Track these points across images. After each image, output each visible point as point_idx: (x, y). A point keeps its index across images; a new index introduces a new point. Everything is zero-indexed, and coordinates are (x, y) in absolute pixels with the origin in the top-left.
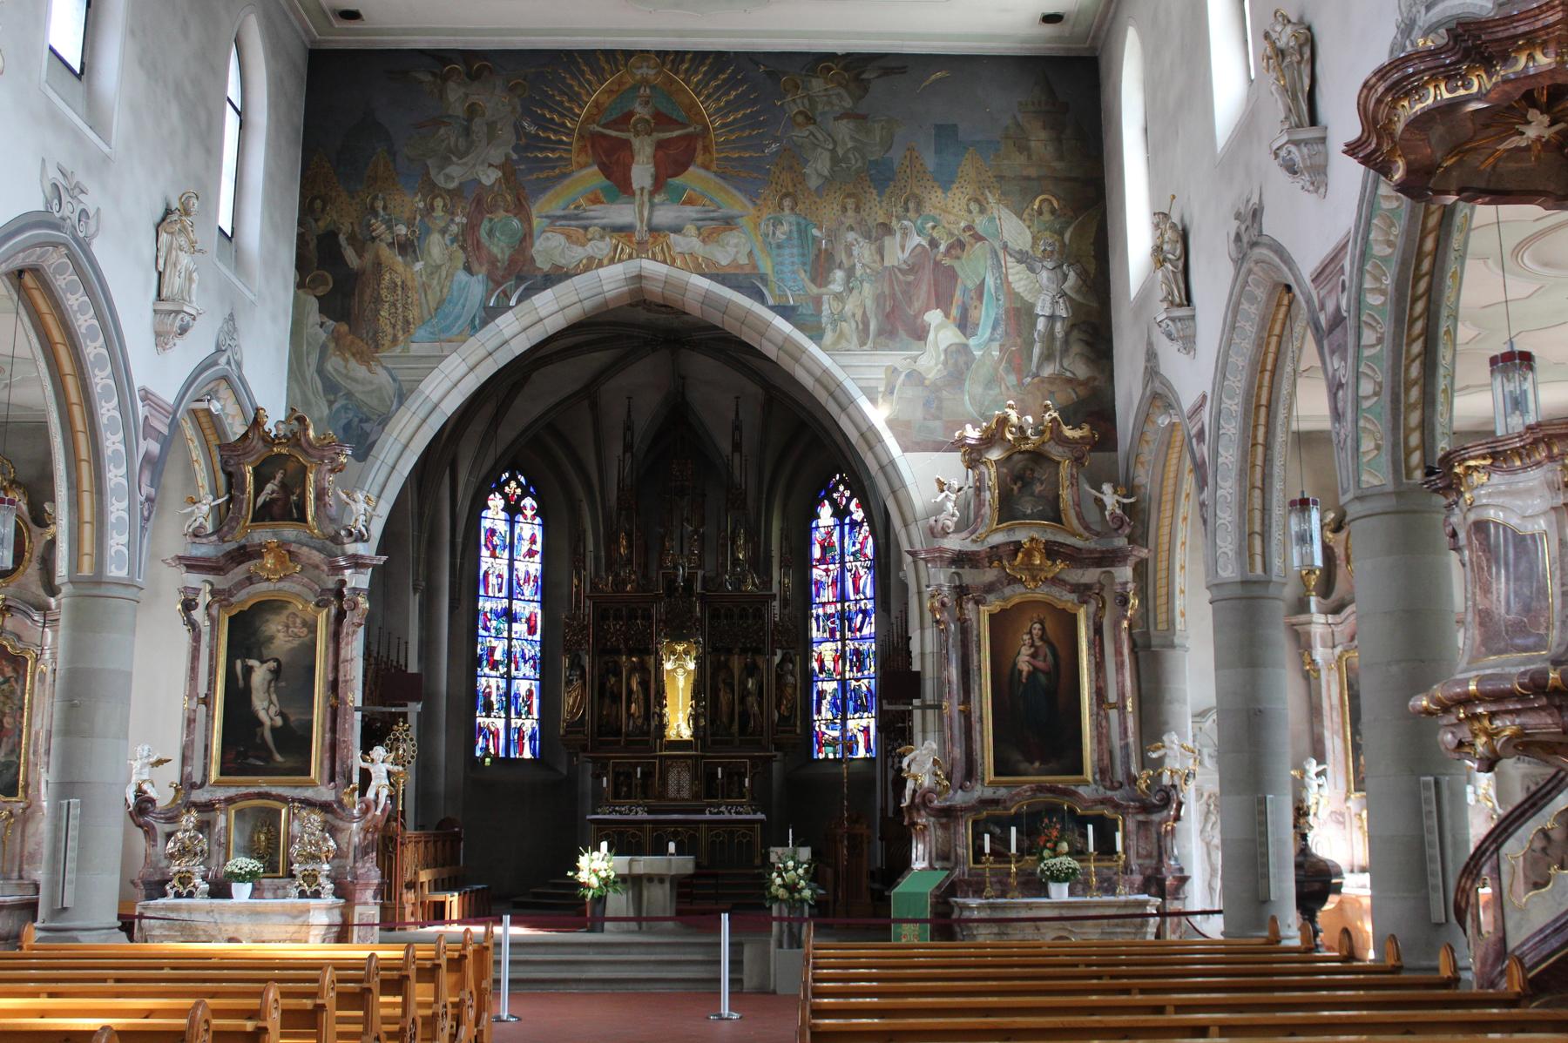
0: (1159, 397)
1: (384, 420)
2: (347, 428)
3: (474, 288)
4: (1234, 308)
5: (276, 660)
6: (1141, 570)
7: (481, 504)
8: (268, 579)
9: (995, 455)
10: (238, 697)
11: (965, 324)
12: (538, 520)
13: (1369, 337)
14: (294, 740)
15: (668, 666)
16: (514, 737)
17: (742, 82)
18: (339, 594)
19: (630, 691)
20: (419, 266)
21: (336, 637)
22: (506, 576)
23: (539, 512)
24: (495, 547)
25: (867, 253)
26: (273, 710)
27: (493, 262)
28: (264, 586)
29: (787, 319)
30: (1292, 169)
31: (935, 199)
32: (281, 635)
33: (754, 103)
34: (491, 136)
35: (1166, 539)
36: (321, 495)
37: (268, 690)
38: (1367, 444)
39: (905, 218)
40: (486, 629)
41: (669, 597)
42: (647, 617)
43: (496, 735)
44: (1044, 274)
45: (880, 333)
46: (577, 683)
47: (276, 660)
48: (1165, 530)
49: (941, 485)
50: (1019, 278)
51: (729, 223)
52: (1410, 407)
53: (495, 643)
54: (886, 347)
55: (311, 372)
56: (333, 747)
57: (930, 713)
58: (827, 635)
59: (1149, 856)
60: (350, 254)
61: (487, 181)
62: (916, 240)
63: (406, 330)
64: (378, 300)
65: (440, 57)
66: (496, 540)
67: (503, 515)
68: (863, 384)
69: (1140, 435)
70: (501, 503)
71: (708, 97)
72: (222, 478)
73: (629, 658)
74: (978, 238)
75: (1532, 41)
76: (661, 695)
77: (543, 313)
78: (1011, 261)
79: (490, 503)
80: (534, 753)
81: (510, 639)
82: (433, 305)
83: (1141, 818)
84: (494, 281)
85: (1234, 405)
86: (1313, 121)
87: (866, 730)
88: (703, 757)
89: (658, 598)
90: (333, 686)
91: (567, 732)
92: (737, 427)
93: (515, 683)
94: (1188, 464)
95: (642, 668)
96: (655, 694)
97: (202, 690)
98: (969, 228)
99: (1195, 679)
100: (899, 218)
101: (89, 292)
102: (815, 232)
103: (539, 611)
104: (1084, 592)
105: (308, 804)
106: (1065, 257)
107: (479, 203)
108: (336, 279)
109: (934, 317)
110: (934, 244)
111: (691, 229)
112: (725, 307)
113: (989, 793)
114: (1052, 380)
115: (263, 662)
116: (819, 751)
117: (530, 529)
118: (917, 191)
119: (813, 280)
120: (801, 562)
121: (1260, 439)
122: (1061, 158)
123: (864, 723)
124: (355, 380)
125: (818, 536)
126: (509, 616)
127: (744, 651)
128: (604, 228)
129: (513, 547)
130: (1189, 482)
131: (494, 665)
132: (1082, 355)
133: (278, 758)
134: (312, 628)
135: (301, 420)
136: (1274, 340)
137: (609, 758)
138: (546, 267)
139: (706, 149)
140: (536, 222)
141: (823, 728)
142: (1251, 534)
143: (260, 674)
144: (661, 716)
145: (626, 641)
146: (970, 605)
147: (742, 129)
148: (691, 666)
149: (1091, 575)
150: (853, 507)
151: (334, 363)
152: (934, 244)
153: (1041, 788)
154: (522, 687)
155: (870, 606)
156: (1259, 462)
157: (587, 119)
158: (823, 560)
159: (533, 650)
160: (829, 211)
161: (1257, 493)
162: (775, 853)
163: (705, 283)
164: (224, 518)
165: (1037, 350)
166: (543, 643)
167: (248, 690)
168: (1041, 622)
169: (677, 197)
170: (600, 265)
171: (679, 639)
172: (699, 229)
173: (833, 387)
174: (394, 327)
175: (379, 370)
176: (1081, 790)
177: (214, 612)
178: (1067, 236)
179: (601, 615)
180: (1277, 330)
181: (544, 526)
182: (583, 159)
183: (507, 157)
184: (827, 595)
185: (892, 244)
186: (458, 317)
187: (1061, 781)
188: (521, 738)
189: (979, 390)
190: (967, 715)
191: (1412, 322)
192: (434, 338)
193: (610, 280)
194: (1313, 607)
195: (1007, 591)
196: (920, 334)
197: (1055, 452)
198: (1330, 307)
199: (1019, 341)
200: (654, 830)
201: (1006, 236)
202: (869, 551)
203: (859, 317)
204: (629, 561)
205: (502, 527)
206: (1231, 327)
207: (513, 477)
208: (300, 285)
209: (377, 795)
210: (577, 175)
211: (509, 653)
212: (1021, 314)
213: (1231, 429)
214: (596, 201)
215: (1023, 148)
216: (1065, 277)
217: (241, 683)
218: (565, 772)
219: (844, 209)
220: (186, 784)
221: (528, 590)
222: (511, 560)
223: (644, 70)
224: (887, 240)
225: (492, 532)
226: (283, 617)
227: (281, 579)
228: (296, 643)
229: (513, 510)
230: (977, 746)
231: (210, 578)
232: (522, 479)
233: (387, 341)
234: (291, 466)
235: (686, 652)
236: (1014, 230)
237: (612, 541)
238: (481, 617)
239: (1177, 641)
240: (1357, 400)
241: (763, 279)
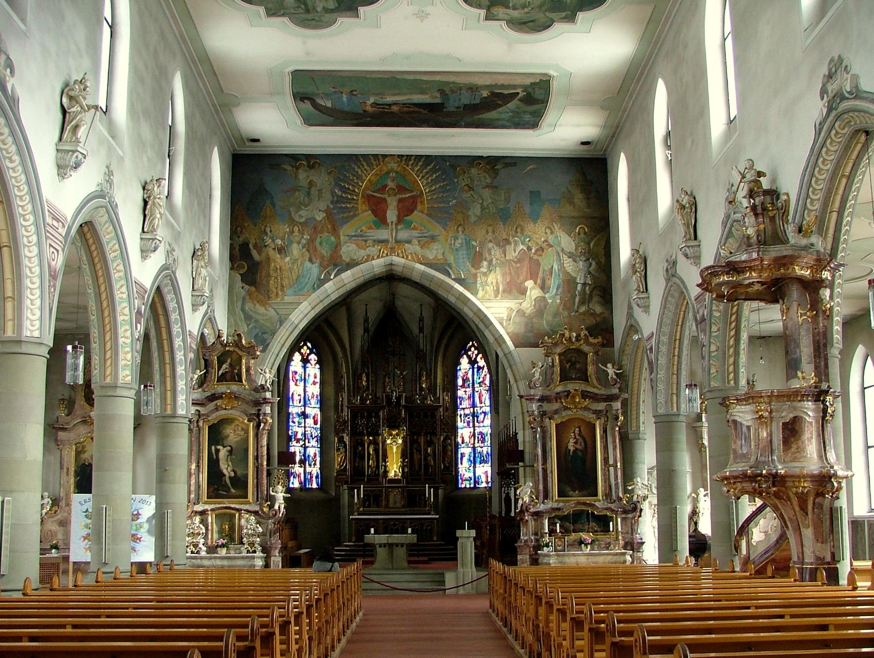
0: (633, 328)
1: (273, 333)
2: (256, 337)
3: (314, 270)
4: (665, 299)
6: (625, 404)
9: (559, 350)
10: (213, 463)
11: (544, 287)
12: (318, 366)
13: (714, 328)
14: (240, 483)
15: (389, 442)
16: (308, 477)
17: (437, 171)
18: (258, 415)
19: (369, 454)
20: (288, 259)
21: (257, 436)
23: (319, 362)
25: (498, 253)
26: (229, 469)
27: (323, 257)
28: (223, 412)
29: (461, 285)
30: (686, 256)
31: (530, 227)
33: (444, 180)
34: (320, 197)
35: (636, 389)
36: (248, 370)
38: (713, 370)
39: (516, 236)
40: (294, 422)
41: (389, 407)
43: (299, 476)
44: (581, 263)
45: (504, 291)
48: (636, 385)
49: (534, 365)
50: (569, 265)
51: (433, 239)
52: (730, 356)
54: (507, 298)
55: (238, 310)
56: (258, 485)
57: (528, 469)
58: (466, 424)
59: (627, 533)
60: (254, 253)
61: (319, 219)
62: (522, 247)
63: (282, 291)
64: (268, 276)
65: (294, 158)
66: (297, 377)
67: (301, 364)
68: (497, 316)
69: (624, 343)
71: (423, 177)
72: (203, 362)
73: (368, 438)
74: (552, 246)
75: (751, 269)
76: (385, 456)
77: (346, 282)
78: (565, 258)
81: (305, 427)
82: (295, 277)
83: (623, 516)
84: (323, 267)
85: (664, 339)
86: (696, 238)
89: (383, 408)
90: (257, 458)
91: (338, 475)
92: (421, 320)
93: (308, 450)
94: (646, 365)
95: (375, 443)
96: (382, 455)
98: (546, 241)
99: (647, 456)
100: (513, 237)
101: (175, 293)
102: (474, 243)
103: (319, 413)
104: (598, 413)
105: (248, 511)
106: (589, 255)
107: (316, 229)
108: (247, 264)
109: (529, 284)
110: (529, 249)
111: (415, 241)
112: (432, 278)
113: (555, 505)
114: (584, 314)
117: (314, 370)
118: (522, 223)
119: (473, 266)
120: (452, 388)
121: (676, 354)
122: (589, 207)
124: (258, 314)
125: (460, 374)
126: (304, 415)
127: (426, 434)
128: (374, 241)
129: (307, 381)
130: (645, 374)
131: (298, 441)
132: (599, 302)
133: (233, 491)
134: (247, 432)
135: (239, 335)
136: (682, 313)
138: (348, 260)
139: (422, 202)
140: (342, 238)
141: (464, 472)
142: (672, 394)
143: (223, 452)
144: (385, 467)
146: (547, 420)
147: (440, 192)
148: (400, 441)
149: (601, 406)
150: (478, 359)
151: (249, 306)
152: (529, 249)
153: (579, 503)
154: (311, 451)
155: (488, 409)
156: (676, 363)
157: (365, 188)
158: (463, 386)
160: (481, 232)
161: (675, 376)
162: (459, 533)
163: (422, 268)
164: (202, 382)
165: (577, 300)
168: (579, 428)
169: (408, 226)
170: (373, 259)
171: (392, 427)
172: (419, 241)
173: (482, 317)
174: (276, 288)
175: (270, 309)
176: (596, 504)
178: (592, 245)
179: (354, 416)
180: (683, 309)
181: (321, 370)
182: (364, 207)
183: (328, 206)
184: (466, 404)
185: (510, 249)
186: (307, 284)
187: (588, 499)
188: (311, 477)
189: (550, 318)
190: (545, 470)
191: (731, 323)
192: (296, 294)
193: (378, 266)
194: (704, 419)
195: (564, 413)
196: (523, 292)
197: (585, 348)
198: (701, 312)
199: (569, 295)
200: (384, 523)
201: (563, 245)
202: (487, 382)
203: (494, 284)
204: (368, 388)
205: (300, 370)
206: (664, 307)
207: (305, 344)
208: (232, 269)
210: (361, 215)
211: (305, 434)
212: (569, 282)
213: (663, 349)
214: (370, 228)
215: (571, 202)
216: (591, 264)
219: (487, 232)
221: (314, 402)
222: (305, 386)
223: (392, 164)
224: (508, 247)
225: (296, 373)
228: (239, 438)
229: (305, 361)
230: (550, 484)
231: (198, 408)
232: (309, 345)
233: (273, 295)
234: (235, 356)
235: (397, 435)
236: (567, 242)
237: (357, 377)
239: (641, 436)
240: (710, 352)
241: (450, 265)
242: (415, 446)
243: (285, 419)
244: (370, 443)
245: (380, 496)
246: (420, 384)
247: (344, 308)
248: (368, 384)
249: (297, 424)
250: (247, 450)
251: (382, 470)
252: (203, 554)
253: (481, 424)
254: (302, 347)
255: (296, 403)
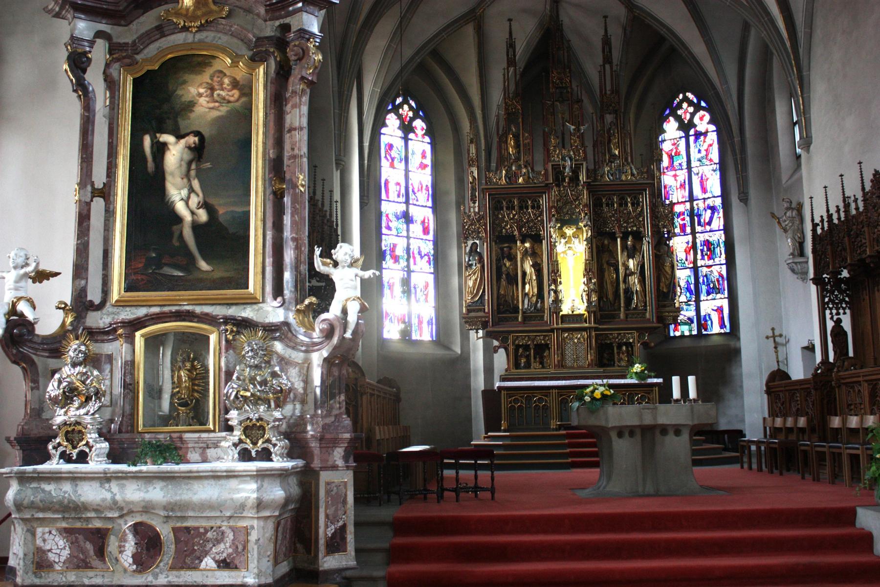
5: (197, 134)
7: (379, 123)
8: (185, 29)
10: (148, 183)
12: (427, 139)
14: (224, 240)
18: (281, 43)
19: (524, 274)
21: (278, 101)
22: (403, 184)
23: (430, 132)
24: (393, 159)
26: (194, 201)
28: (179, 38)
32: (203, 101)
37: (187, 175)
40: (389, 228)
41: (558, 186)
42: (537, 207)
46: (476, 267)
47: (197, 134)
53: (395, 240)
66: (394, 153)
67: (400, 133)
70: (397, 123)
73: (523, 242)
79: (387, 122)
80: (432, 336)
81: (408, 237)
87: (720, 310)
88: (596, 329)
89: (547, 187)
91: (469, 311)
95: (534, 254)
96: (548, 274)
97: (99, 178)
115: (179, 137)
116: (675, 330)
117: (420, 145)
123: (718, 303)
125: (666, 147)
126: (407, 218)
131: (396, 259)
133: (203, 265)
134: (246, 90)
137: (510, 332)
143: (176, 153)
144: (556, 292)
145: (520, 230)
150: (696, 120)
155: (718, 202)
158: (671, 166)
159: (428, 248)
166: (436, 243)
167: (160, 175)
177: (114, 71)
179: (496, 207)
181: (433, 144)
188: (420, 322)
202: (715, 155)
204: (518, 159)
205: (399, 143)
207: (406, 101)
209: (345, 312)
211: (408, 249)
217: (150, 165)
218: (459, 352)
220: (81, 305)
221: (423, 198)
222: (407, 171)
225: (390, 147)
226: (206, 77)
227: (201, 28)
228: (224, 110)
229: (407, 128)
232: (413, 104)
235: (575, 236)
238: (384, 218)
242: (605, 257)
243: (373, 217)
244: (525, 253)
245: (547, 347)
246: (610, 150)
247: (470, 30)
248: (519, 152)
249: (394, 232)
250: (246, 144)
251: (549, 299)
252: (97, 464)
253: (708, 228)
254: (401, 106)
255: (393, 195)
